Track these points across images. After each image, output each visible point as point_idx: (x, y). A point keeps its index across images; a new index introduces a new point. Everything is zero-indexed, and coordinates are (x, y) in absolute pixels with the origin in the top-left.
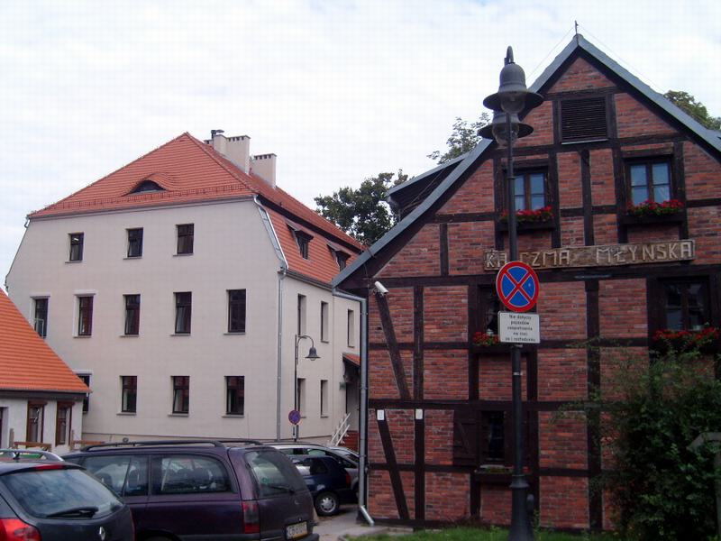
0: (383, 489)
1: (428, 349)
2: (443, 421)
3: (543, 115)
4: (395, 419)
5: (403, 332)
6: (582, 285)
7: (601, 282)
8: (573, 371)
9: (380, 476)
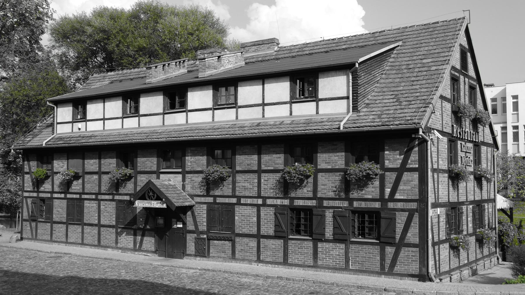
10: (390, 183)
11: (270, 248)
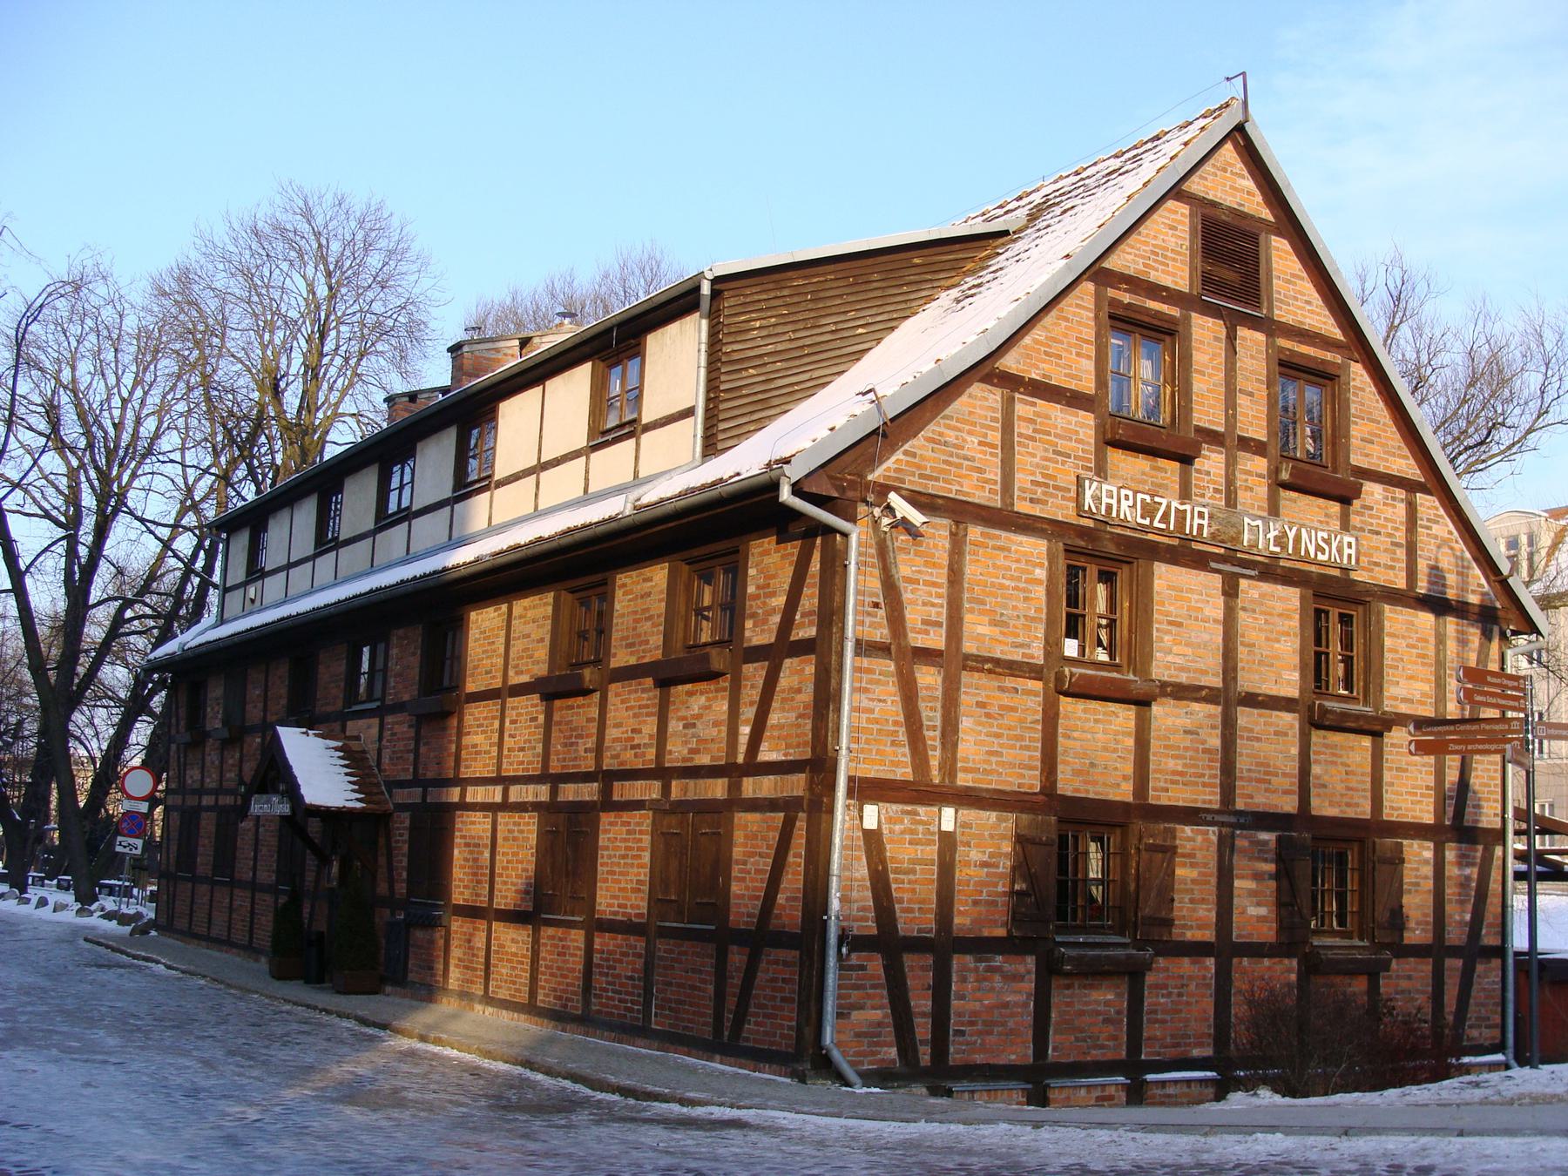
0: (869, 997)
1: (972, 669)
2: (991, 836)
3: (1175, 229)
4: (897, 827)
5: (924, 622)
6: (1217, 580)
7: (1243, 583)
8: (1201, 747)
9: (863, 968)
10: (751, 704)
11: (507, 953)
